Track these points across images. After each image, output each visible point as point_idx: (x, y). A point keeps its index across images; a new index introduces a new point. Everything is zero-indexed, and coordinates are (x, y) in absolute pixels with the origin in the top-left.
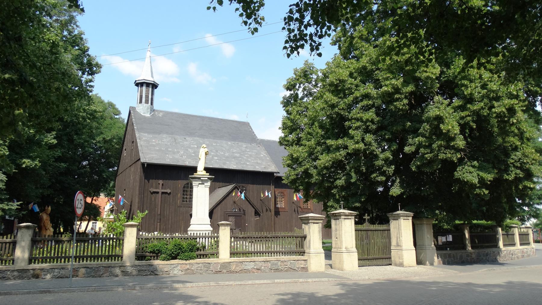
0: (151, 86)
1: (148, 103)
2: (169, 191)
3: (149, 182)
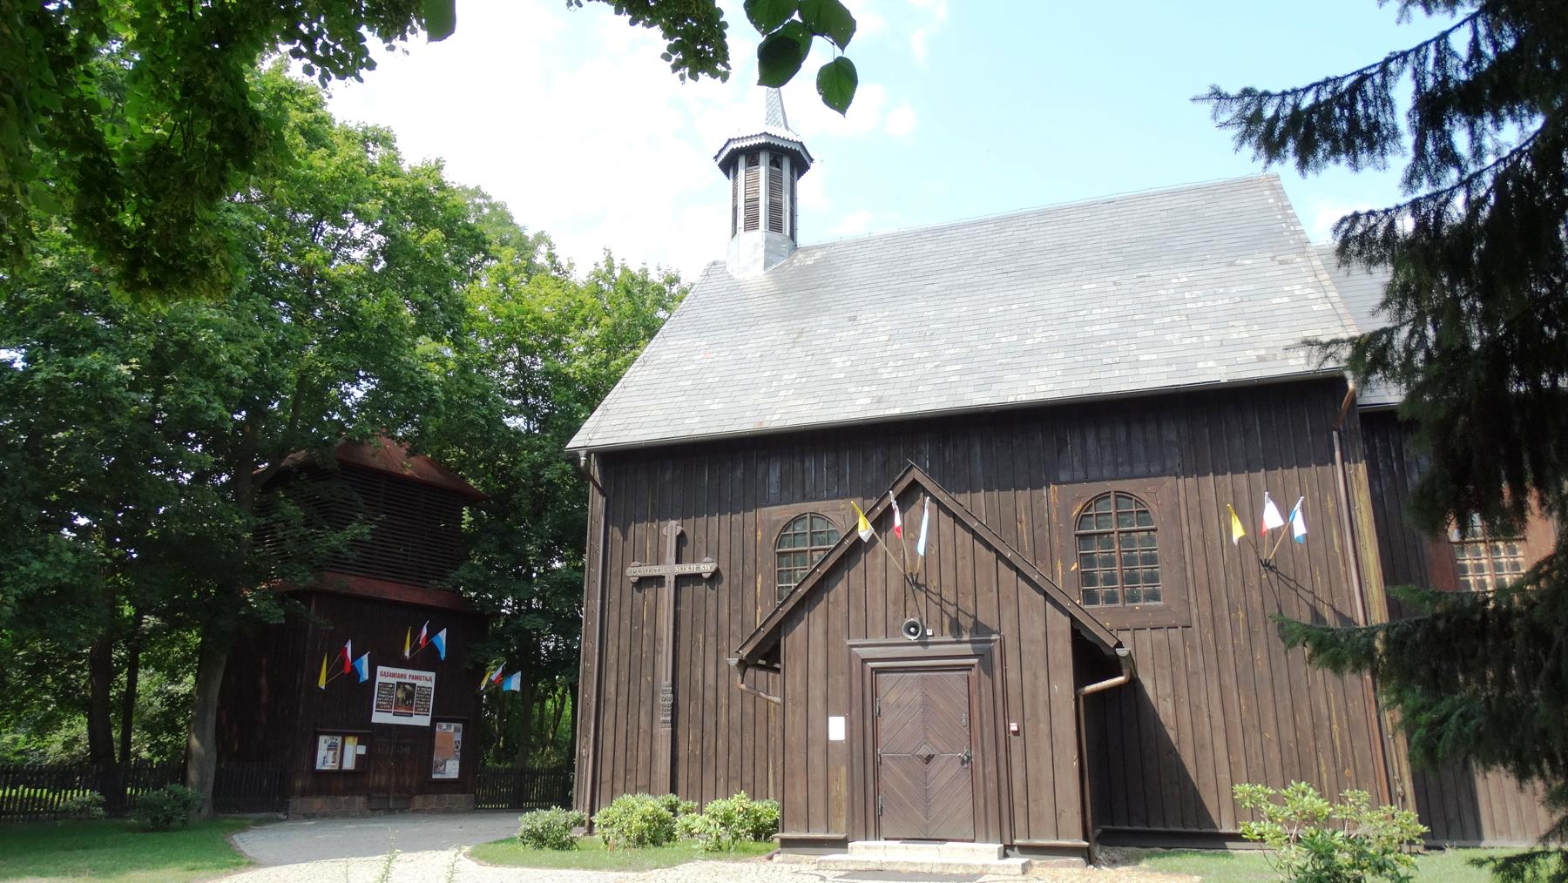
0: (764, 159)
1: (752, 223)
2: (706, 568)
3: (625, 538)
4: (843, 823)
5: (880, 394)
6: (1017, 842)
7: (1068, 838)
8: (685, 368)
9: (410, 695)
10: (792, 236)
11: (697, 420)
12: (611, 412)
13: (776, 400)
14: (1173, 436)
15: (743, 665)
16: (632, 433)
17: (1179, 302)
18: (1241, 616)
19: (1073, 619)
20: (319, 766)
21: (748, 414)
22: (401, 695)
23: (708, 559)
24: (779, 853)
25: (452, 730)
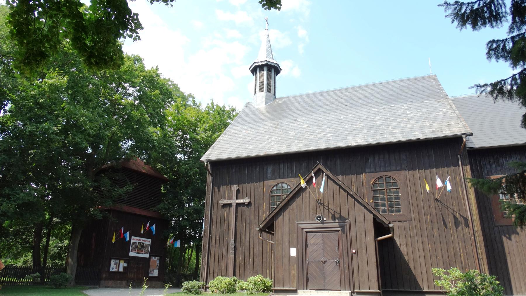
0: (265, 69)
1: (261, 90)
2: (246, 201)
3: (219, 191)
4: (295, 284)
5: (306, 143)
6: (356, 290)
7: (373, 289)
8: (240, 135)
9: (142, 247)
10: (275, 94)
11: (244, 151)
12: (215, 149)
13: (270, 145)
14: (404, 157)
15: (261, 230)
16: (222, 155)
17: (405, 114)
18: (429, 217)
19: (374, 215)
20: (111, 270)
21: (261, 149)
22: (139, 246)
23: (247, 198)
24: (273, 294)
25: (156, 259)
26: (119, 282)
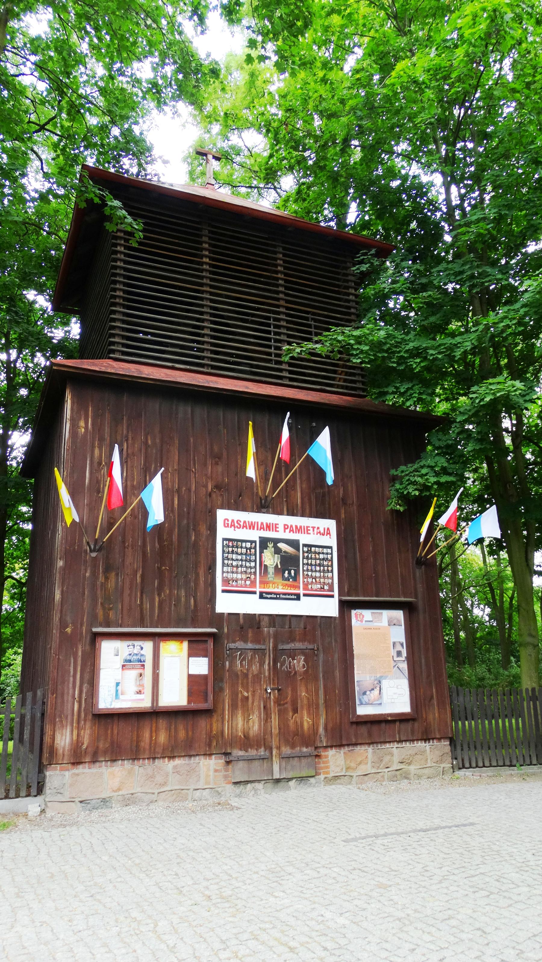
25: (385, 623)
26: (169, 765)
